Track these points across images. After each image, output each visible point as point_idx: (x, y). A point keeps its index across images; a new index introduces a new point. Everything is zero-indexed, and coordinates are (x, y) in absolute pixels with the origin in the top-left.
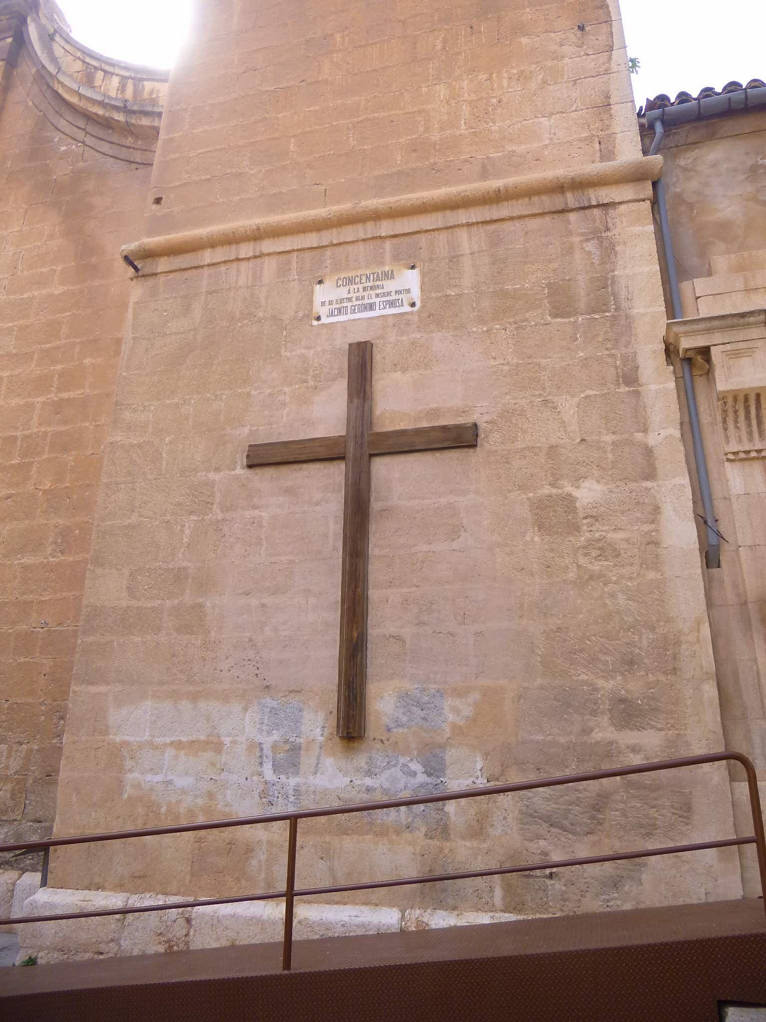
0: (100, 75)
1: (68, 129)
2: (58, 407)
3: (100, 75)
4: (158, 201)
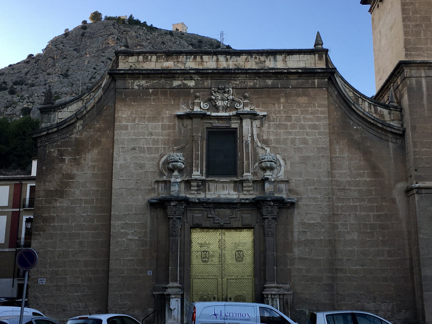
0: (360, 100)
1: (356, 120)
2: (379, 216)
3: (360, 100)
4: (416, 170)
